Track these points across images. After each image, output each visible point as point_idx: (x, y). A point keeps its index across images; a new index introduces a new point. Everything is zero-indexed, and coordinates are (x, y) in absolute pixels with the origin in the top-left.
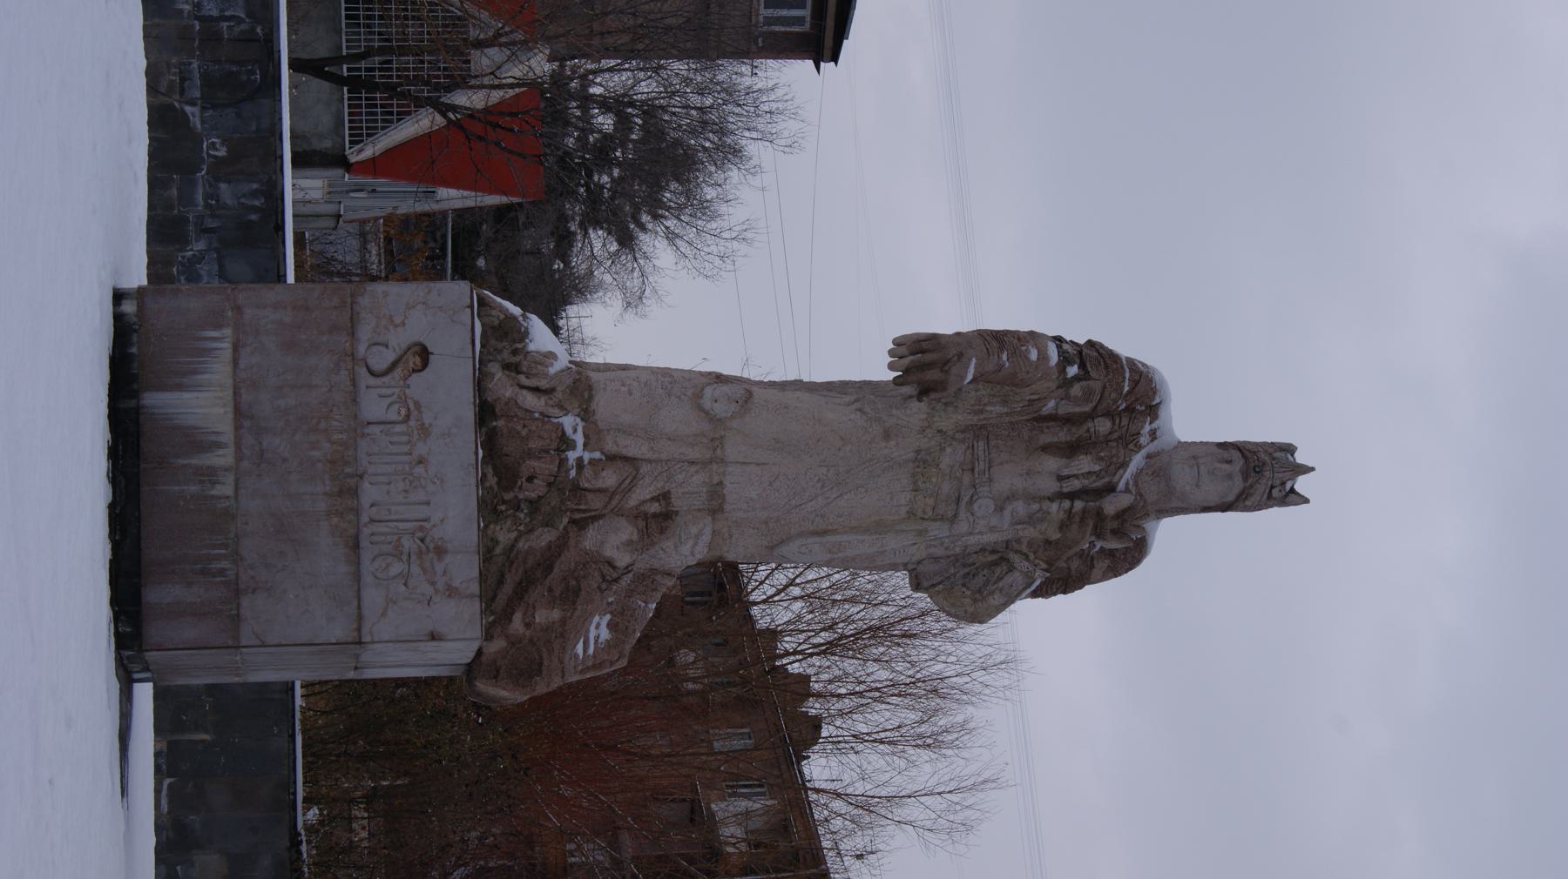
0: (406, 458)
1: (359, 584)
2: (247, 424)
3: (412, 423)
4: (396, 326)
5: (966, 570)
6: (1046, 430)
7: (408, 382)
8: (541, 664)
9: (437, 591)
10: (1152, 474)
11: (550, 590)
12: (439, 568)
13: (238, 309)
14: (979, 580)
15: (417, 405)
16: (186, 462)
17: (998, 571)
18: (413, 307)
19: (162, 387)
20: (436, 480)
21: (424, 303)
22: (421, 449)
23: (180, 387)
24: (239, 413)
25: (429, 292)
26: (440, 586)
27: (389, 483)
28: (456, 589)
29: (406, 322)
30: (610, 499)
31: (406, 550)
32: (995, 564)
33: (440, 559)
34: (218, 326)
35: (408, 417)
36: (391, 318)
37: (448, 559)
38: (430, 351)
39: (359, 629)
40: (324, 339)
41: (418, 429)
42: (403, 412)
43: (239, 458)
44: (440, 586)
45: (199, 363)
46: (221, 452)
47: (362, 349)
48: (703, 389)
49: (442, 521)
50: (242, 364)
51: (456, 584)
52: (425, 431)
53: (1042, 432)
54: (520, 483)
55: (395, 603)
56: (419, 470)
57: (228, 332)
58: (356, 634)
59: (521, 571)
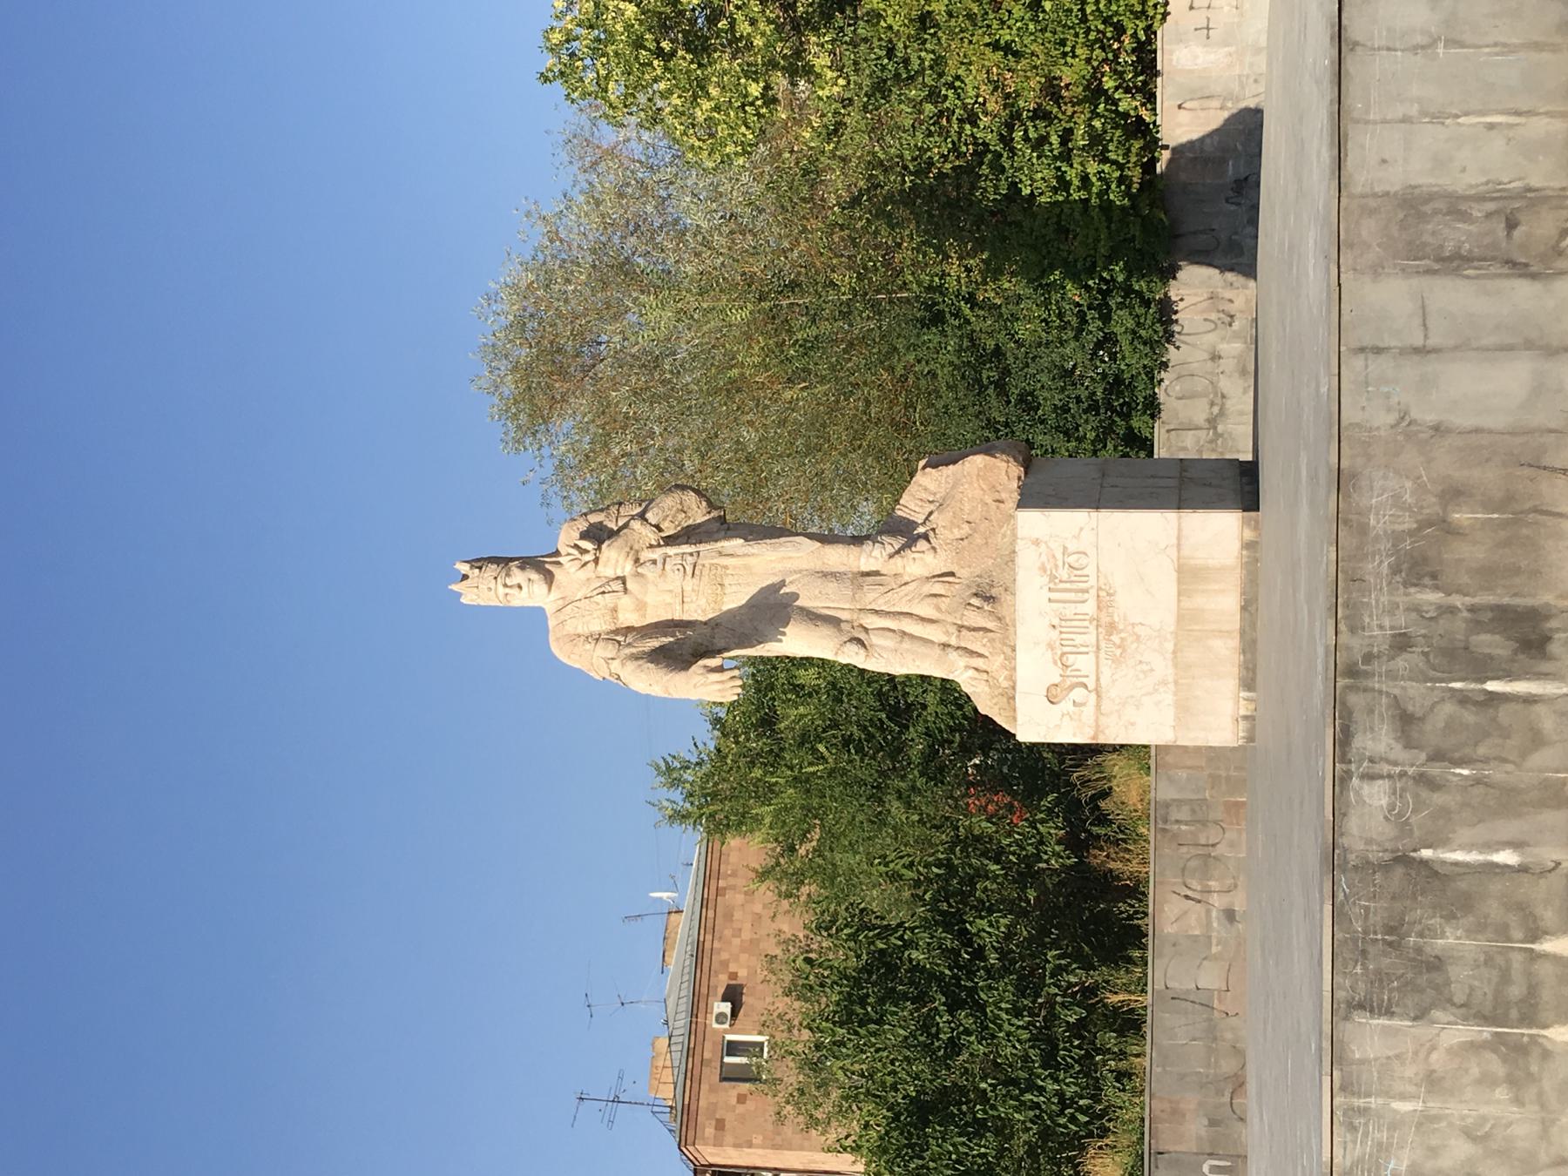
0: (1063, 630)
3: (1059, 653)
12: (1044, 558)
22: (1054, 634)
28: (1033, 544)
33: (1043, 564)
42: (1064, 659)
49: (1041, 588)
51: (1034, 547)
52: (1051, 647)
55: (1074, 536)
56: (1056, 622)
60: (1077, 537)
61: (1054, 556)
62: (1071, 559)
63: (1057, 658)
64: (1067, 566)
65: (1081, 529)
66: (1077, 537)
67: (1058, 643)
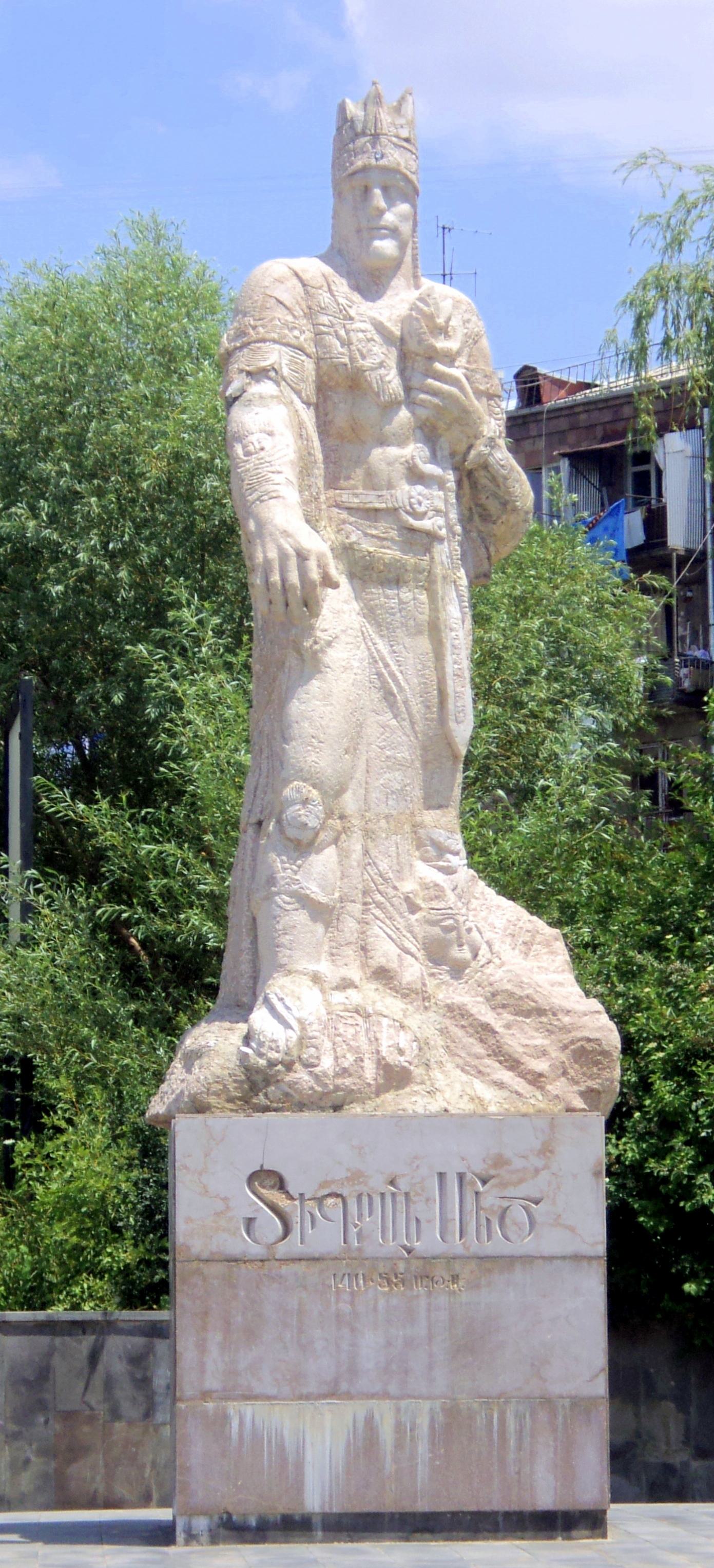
1: (536, 1258)
2: (344, 1386)
3: (345, 1192)
4: (228, 1208)
5: (476, 518)
6: (330, 417)
7: (296, 1196)
8: (589, 1040)
9: (546, 1167)
10: (377, 284)
11: (508, 1026)
12: (518, 1163)
13: (206, 1395)
14: (493, 506)
15: (323, 1185)
16: (389, 1458)
17: (483, 481)
18: (205, 1187)
19: (299, 1487)
20: (415, 1165)
21: (200, 1174)
22: (378, 1183)
23: (300, 1467)
24: (332, 1393)
25: (186, 1167)
26: (539, 1163)
27: (418, 1220)
29: (222, 1196)
30: (408, 952)
31: (498, 1202)
32: (474, 485)
33: (507, 1162)
34: (224, 1418)
35: (337, 1195)
36: (217, 1214)
37: (508, 1153)
38: (258, 1168)
39: (590, 1258)
40: (242, 1294)
41: (354, 1184)
42: (330, 1201)
43: (386, 1395)
44: (539, 1163)
45: (269, 1442)
46: (377, 1417)
47: (256, 1250)
48: (289, 839)
50: (273, 1391)
51: (537, 1145)
52: (356, 1176)
53: (330, 422)
54: (406, 1064)
56: (403, 1184)
57: (232, 1407)
58: (595, 1263)
59: (487, 1061)
60: (557, 1221)
61: (521, 1181)
62: (518, 1214)
63: (334, 1188)
64: (505, 1204)
65: (572, 1229)
66: (557, 1221)
67: (365, 1189)
